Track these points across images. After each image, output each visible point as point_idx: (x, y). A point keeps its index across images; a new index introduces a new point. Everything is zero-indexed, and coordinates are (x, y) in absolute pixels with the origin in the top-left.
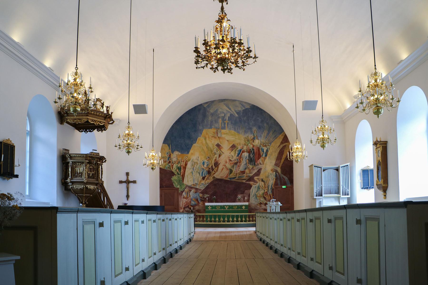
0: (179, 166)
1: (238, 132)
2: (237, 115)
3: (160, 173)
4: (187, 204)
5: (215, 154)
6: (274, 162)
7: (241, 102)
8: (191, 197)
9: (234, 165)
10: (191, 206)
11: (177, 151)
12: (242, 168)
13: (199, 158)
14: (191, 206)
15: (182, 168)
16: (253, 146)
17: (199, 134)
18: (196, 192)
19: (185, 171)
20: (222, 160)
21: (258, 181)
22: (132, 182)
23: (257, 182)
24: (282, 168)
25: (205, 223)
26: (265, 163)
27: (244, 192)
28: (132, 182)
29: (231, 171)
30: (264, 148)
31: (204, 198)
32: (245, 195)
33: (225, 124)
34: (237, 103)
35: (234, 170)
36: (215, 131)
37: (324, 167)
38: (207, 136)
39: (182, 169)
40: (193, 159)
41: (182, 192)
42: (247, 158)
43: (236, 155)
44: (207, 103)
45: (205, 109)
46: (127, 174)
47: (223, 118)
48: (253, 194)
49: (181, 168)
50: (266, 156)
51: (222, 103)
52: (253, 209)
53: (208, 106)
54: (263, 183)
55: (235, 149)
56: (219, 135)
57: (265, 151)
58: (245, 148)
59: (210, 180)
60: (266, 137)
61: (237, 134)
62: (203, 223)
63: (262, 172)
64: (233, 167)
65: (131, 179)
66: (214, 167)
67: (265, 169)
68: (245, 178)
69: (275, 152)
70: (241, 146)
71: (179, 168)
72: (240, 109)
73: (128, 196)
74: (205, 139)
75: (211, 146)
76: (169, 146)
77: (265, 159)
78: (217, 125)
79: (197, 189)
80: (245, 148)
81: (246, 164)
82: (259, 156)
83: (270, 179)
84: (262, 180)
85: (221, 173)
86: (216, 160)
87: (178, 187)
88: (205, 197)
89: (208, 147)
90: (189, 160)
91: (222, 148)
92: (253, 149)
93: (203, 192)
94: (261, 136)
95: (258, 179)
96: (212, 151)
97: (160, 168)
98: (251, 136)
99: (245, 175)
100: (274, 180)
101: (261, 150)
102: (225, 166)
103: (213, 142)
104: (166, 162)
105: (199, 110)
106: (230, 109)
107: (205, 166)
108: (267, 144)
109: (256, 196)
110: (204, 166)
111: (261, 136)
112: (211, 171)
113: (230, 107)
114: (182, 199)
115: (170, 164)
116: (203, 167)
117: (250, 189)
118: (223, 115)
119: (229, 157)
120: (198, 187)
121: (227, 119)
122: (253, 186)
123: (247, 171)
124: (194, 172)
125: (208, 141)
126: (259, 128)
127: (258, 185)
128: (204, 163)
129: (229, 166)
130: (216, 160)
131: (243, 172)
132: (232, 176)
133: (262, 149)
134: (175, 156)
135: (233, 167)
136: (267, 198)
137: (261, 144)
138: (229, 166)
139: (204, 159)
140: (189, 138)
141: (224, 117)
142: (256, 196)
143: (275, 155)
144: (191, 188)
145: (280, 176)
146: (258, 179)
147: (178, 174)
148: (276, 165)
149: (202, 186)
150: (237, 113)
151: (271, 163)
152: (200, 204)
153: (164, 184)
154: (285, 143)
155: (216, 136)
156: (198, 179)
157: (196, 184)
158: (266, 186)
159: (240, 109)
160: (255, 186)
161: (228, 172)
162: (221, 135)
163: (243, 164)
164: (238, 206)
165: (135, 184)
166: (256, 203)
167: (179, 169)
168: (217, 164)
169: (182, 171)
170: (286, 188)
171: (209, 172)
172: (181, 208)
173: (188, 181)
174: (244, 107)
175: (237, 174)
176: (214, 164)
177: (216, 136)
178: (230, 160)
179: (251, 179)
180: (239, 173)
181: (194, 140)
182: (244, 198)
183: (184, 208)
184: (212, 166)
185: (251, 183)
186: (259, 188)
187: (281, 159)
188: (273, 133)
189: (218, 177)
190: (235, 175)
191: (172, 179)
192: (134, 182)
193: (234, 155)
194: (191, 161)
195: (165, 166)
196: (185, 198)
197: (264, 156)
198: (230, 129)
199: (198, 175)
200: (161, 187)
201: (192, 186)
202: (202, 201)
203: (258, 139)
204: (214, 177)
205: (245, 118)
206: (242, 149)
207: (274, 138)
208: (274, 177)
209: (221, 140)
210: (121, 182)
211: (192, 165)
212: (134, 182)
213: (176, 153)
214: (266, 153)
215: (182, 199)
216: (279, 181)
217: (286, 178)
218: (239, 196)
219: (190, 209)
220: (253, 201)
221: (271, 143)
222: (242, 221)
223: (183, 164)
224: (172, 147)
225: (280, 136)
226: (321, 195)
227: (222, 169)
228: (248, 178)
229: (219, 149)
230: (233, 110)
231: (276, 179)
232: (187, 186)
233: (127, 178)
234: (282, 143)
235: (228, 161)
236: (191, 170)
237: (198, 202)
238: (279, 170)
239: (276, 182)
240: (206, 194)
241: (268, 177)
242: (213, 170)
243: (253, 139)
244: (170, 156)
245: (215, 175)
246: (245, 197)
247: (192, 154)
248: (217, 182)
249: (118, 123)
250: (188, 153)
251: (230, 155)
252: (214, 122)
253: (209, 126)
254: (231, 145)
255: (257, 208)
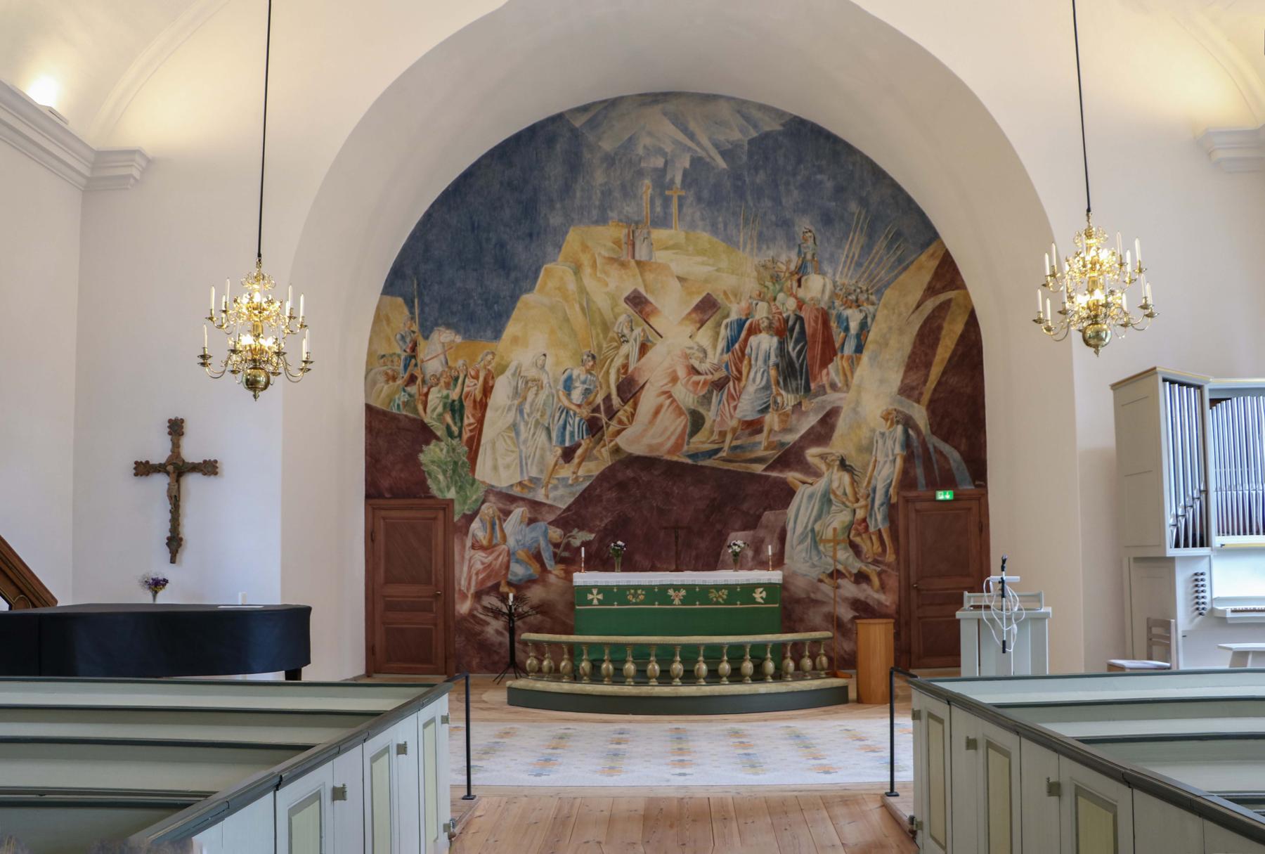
0: (454, 395)
1: (729, 241)
2: (722, 164)
3: (369, 428)
4: (488, 577)
5: (623, 339)
6: (895, 378)
7: (742, 107)
8: (511, 542)
9: (710, 392)
10: (509, 584)
11: (448, 326)
12: (746, 407)
13: (550, 361)
14: (509, 584)
15: (468, 404)
16: (801, 304)
17: (550, 249)
18: (532, 521)
19: (481, 422)
20: (657, 369)
21: (823, 467)
22: (195, 468)
23: (817, 474)
24: (932, 407)
25: (566, 687)
26: (855, 381)
27: (760, 517)
28: (195, 468)
29: (697, 421)
30: (849, 312)
31: (568, 546)
32: (761, 533)
33: (667, 201)
34: (725, 111)
35: (710, 416)
36: (622, 233)
37: (1213, 383)
38: (585, 259)
39: (469, 410)
40: (519, 367)
41: (470, 519)
42: (773, 359)
43: (721, 344)
44: (585, 109)
45: (575, 134)
46: (176, 428)
47: (661, 180)
48: (799, 529)
49: (462, 406)
50: (859, 349)
51: (658, 108)
52: (798, 601)
53: (593, 124)
54: (846, 478)
55: (717, 317)
56: (642, 254)
57: (854, 326)
58: (761, 313)
59: (600, 462)
60: (859, 265)
61: (722, 246)
62: (554, 687)
63: (842, 424)
64: (706, 400)
65: (192, 452)
66: (616, 401)
67: (855, 411)
68: (760, 453)
69: (901, 332)
70: (744, 304)
71: (456, 409)
72: (736, 136)
73: (175, 543)
74: (577, 270)
75: (601, 301)
76: (410, 303)
77: (853, 362)
78: (629, 209)
79: (535, 505)
80: (761, 313)
81: (767, 387)
82: (829, 352)
83: (881, 458)
84: (844, 465)
85: (650, 432)
86: (625, 366)
87: (451, 494)
88: (576, 543)
89: (588, 309)
90: (502, 369)
91: (655, 311)
92: (799, 319)
93: (567, 521)
94: (833, 259)
95: (823, 457)
96: (606, 327)
97: (369, 408)
98: (788, 259)
99: (762, 438)
100: (899, 462)
101: (833, 325)
102: (668, 394)
103: (612, 286)
104: (394, 379)
105: (551, 141)
106: (692, 136)
107: (577, 395)
108: (863, 297)
109: (815, 539)
110: (569, 395)
111: (833, 259)
112: (603, 417)
113: (692, 126)
114: (469, 553)
115: (413, 389)
116: (566, 402)
117: (786, 504)
118: (660, 162)
119: (687, 357)
120: (540, 496)
121: (678, 180)
122: (802, 493)
123: (772, 420)
124: (522, 427)
125: (589, 282)
126: (827, 220)
127: (821, 485)
128: (568, 385)
129: (686, 396)
130: (625, 366)
131: (754, 427)
132: (701, 442)
133: (839, 316)
134: (439, 349)
135: (706, 400)
136: (865, 547)
137: (834, 295)
138: (686, 396)
139: (568, 364)
140: (504, 265)
141: (663, 171)
142: (815, 539)
143: (902, 345)
144: (509, 499)
145: (924, 444)
146: (823, 457)
147: (450, 433)
148: (907, 391)
149: (561, 491)
150: (723, 154)
151: (882, 381)
152: (552, 579)
153: (385, 483)
154: (944, 289)
155: (625, 256)
156: (542, 457)
157: (531, 480)
158: (862, 492)
159: (736, 134)
160: (809, 489)
161: (682, 423)
162: (651, 252)
163: (751, 388)
164: (731, 588)
165: (211, 480)
166: (814, 574)
167: (453, 411)
168: (629, 389)
169: (469, 419)
170: (957, 498)
171: (594, 427)
172: (464, 596)
173: (495, 468)
174: (755, 127)
175: (723, 434)
176: (619, 388)
177: (625, 256)
178: (694, 371)
179: (790, 457)
180: (734, 430)
181: (525, 279)
182: (758, 547)
183: (478, 596)
184: (608, 398)
185: (792, 476)
186: (827, 499)
187: (928, 365)
188: (889, 247)
189: (638, 450)
190: (715, 437)
191: (422, 457)
192: (209, 468)
193: (708, 346)
194: (509, 373)
195: (391, 400)
196: (482, 548)
197: (849, 349)
198: (692, 226)
199: (542, 437)
200: (373, 493)
201: (516, 491)
202: (559, 560)
203: (823, 274)
204: (617, 450)
205: (761, 177)
206: (748, 315)
207: (892, 268)
208: (898, 450)
209: (650, 276)
210: (143, 469)
211: (516, 393)
212: (209, 468)
213: (444, 336)
214: (858, 336)
215: (469, 553)
216: (920, 467)
217: (954, 456)
218: (738, 541)
219: (504, 598)
220: (803, 564)
221: (879, 292)
222: (759, 676)
223: (473, 387)
224: (422, 312)
225: (923, 257)
226: (1204, 541)
227: (657, 412)
228: (774, 454)
229: (645, 317)
230: (705, 141)
231: (909, 459)
232: (490, 490)
233: (176, 446)
234: (931, 291)
235: (681, 373)
236: (510, 417)
237: (543, 565)
238: (920, 414)
239: (905, 472)
240: (581, 529)
241: (868, 449)
242: (611, 413)
243: (800, 274)
244: (414, 349)
245: (621, 441)
246: (762, 541)
247: (515, 340)
248: (632, 474)
249: (136, 173)
250: (497, 335)
251: (690, 343)
252: (617, 194)
253: (595, 212)
254: (697, 300)
255: (819, 597)
